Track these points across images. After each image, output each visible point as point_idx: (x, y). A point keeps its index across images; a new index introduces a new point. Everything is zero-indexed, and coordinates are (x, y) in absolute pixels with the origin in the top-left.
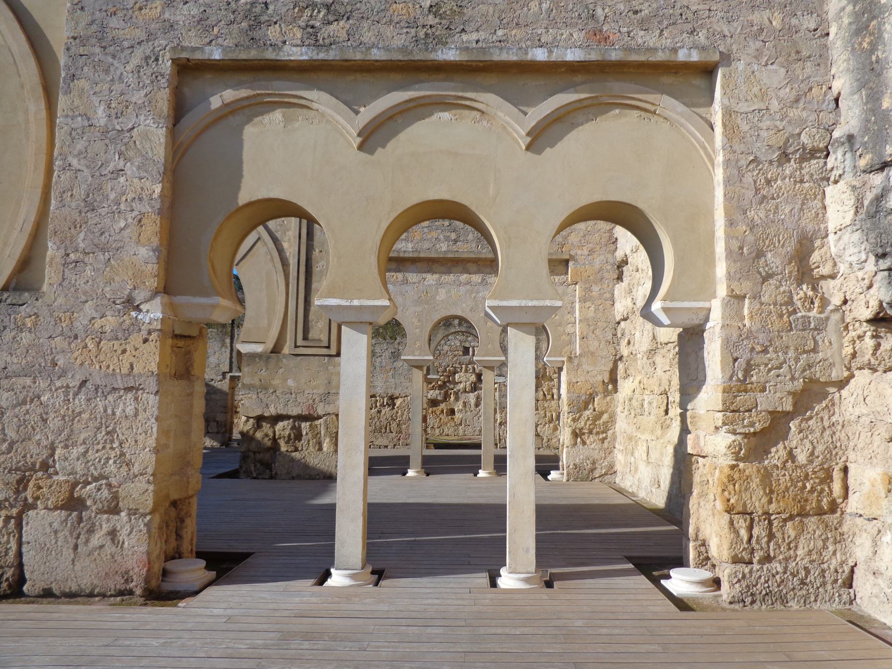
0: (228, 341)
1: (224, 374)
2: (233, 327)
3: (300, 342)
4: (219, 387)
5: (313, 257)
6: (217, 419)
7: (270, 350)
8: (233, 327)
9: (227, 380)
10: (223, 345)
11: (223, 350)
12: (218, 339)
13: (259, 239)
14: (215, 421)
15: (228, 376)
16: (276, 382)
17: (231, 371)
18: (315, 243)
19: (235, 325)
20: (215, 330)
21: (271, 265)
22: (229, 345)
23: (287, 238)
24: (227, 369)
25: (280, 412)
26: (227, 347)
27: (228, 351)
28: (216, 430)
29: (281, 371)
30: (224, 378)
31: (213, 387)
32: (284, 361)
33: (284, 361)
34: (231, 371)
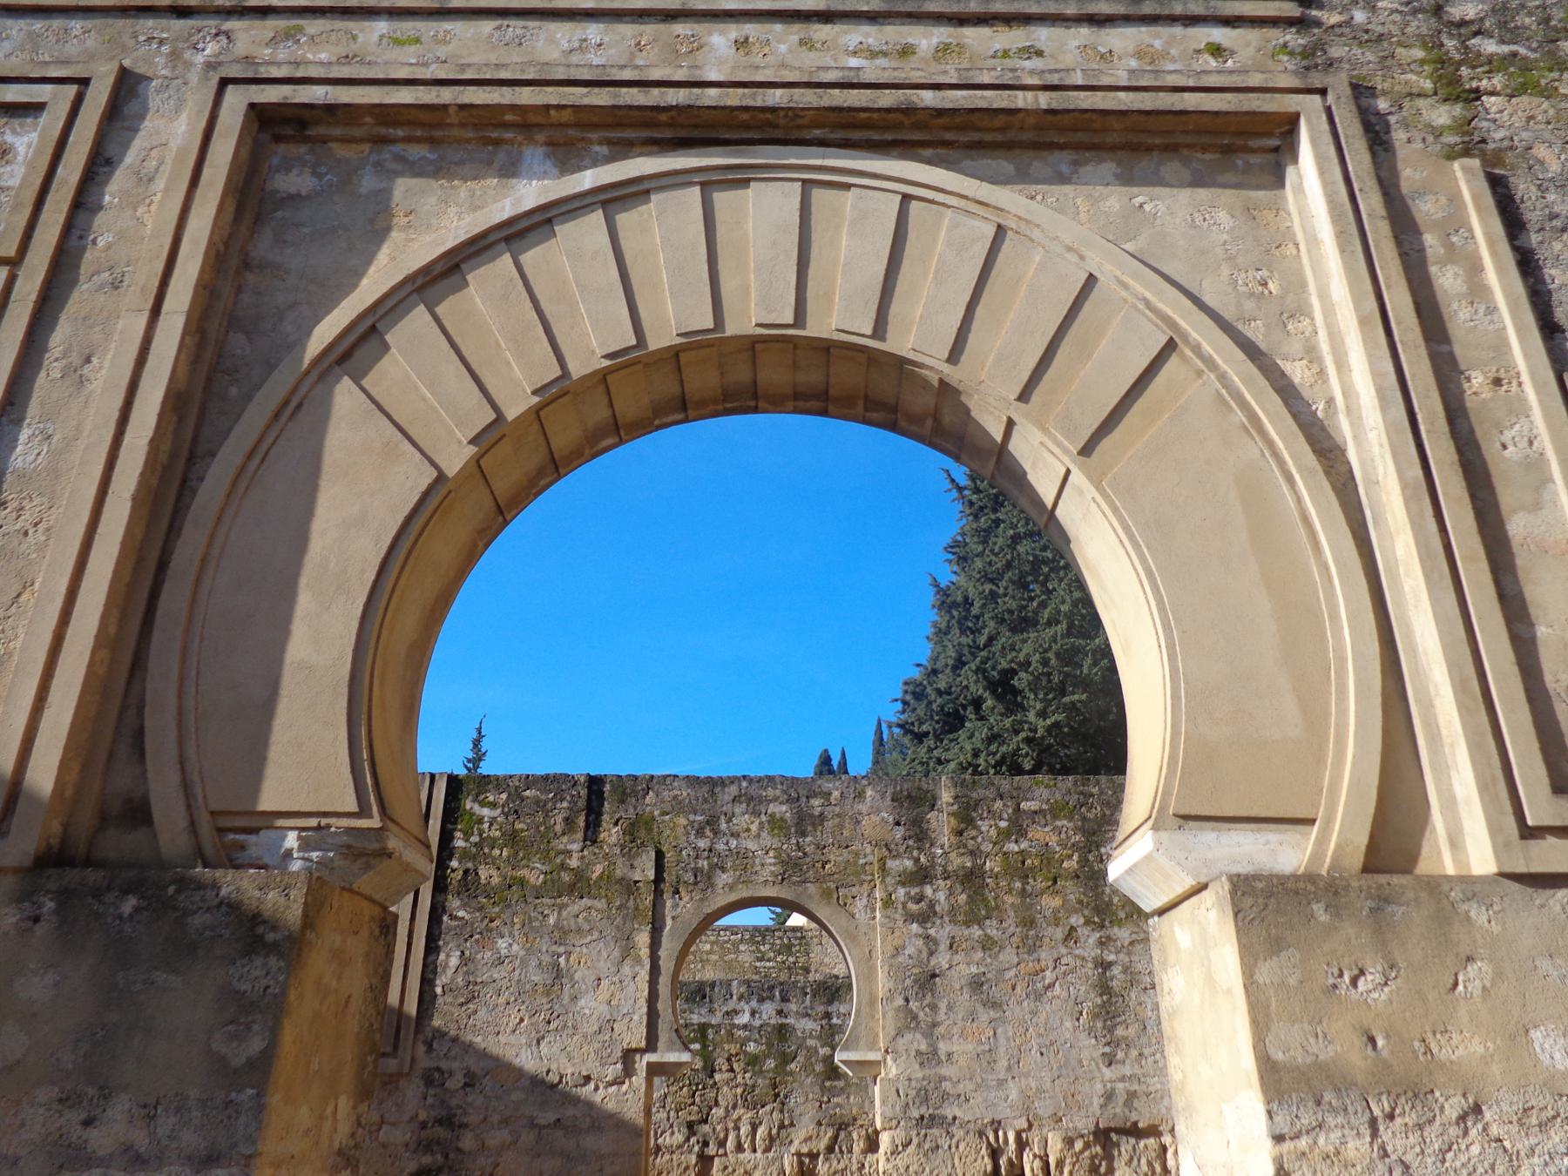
0: (643, 939)
1: (628, 1056)
2: (658, 893)
4: (611, 1106)
5: (1470, 402)
7: (1356, 860)
8: (658, 893)
9: (639, 1080)
10: (628, 951)
11: (626, 970)
12: (610, 932)
13: (1170, 346)
15: (642, 1062)
16: (1465, 1047)
17: (651, 1044)
18: (1458, 350)
19: (666, 887)
20: (601, 904)
21: (1252, 450)
22: (645, 952)
23: (1296, 347)
24: (638, 1038)
26: (638, 960)
27: (644, 974)
29: (1475, 977)
30: (628, 1071)
31: (590, 1105)
32: (1479, 915)
33: (1479, 915)
34: (651, 1044)
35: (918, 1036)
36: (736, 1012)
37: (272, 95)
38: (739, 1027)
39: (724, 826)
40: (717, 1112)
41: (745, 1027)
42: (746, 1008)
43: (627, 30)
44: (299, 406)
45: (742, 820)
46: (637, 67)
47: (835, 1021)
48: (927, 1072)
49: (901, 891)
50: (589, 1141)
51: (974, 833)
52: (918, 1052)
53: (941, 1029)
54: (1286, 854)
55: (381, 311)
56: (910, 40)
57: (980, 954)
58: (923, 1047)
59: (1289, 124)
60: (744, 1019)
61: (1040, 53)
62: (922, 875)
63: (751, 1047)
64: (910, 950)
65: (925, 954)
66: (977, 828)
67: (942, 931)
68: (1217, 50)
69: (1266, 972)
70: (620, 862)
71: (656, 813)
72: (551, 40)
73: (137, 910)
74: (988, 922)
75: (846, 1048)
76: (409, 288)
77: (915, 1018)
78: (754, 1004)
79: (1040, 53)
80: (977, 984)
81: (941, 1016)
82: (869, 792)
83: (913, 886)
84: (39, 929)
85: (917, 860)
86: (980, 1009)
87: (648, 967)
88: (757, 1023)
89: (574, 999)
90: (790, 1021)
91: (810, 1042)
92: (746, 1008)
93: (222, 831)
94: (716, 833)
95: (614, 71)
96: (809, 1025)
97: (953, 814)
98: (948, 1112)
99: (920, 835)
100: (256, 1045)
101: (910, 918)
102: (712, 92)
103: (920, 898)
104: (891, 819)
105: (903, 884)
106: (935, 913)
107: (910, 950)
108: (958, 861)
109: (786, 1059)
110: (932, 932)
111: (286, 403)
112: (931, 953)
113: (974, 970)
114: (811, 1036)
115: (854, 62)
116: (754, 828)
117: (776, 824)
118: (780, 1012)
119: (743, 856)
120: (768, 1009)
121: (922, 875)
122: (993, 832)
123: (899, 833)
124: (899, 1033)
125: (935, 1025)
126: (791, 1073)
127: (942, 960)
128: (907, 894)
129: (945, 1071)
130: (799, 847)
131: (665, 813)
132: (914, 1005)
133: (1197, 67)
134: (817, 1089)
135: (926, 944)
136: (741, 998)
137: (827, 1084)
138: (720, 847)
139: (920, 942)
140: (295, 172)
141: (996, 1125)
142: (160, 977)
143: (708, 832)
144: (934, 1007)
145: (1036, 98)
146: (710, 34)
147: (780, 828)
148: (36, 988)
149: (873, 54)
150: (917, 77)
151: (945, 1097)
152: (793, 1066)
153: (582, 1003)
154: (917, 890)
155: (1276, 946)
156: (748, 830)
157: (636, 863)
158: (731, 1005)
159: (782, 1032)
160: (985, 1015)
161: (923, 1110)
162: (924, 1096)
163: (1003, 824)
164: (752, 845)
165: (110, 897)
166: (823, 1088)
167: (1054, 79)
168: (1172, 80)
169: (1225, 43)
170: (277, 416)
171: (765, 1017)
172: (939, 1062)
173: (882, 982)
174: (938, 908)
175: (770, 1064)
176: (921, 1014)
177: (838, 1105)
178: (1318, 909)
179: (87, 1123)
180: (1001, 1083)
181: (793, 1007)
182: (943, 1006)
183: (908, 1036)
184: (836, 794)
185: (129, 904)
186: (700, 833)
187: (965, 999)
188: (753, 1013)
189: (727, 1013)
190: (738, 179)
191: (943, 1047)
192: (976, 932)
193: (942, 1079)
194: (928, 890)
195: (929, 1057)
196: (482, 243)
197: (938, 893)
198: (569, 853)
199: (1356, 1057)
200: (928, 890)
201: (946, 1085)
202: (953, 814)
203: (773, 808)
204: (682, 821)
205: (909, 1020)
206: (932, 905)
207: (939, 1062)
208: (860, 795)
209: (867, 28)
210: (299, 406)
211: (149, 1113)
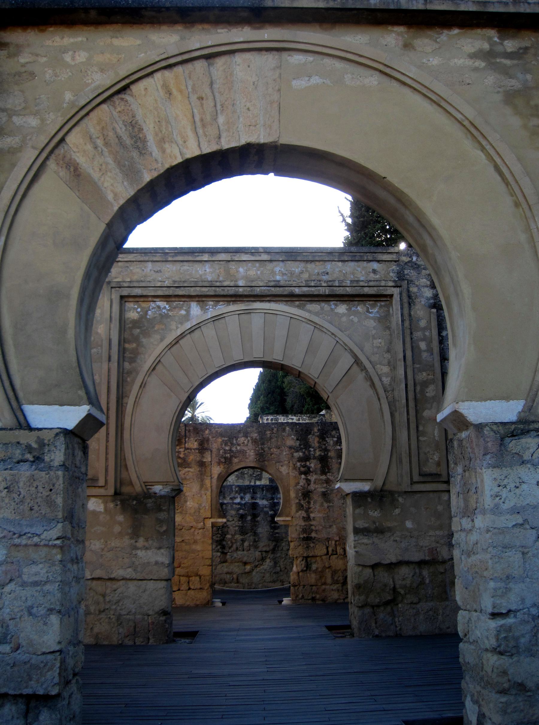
3: (416, 478)
6: (200, 573)
11: (203, 492)
14: (197, 575)
25: (400, 558)
28: (199, 586)
29: (397, 511)
32: (400, 499)
35: (303, 512)
36: (235, 498)
37: (125, 292)
38: (236, 504)
39: (235, 442)
40: (229, 536)
41: (239, 504)
42: (239, 496)
43: (216, 266)
44: (145, 383)
45: (242, 440)
46: (220, 282)
47: (275, 501)
48: (306, 523)
49: (298, 464)
50: (194, 547)
51: (325, 443)
52: (303, 517)
53: (311, 510)
54: (366, 487)
55: (161, 356)
56: (293, 269)
57: (325, 485)
58: (305, 515)
59: (391, 296)
60: (238, 500)
61: (327, 273)
62: (306, 458)
63: (241, 512)
64: (301, 484)
65: (306, 485)
66: (326, 441)
67: (313, 477)
68: (374, 271)
69: (357, 511)
70: (198, 455)
71: (210, 437)
72: (197, 271)
73: (136, 503)
74: (328, 474)
75: (279, 516)
76: (167, 349)
77: (302, 506)
78: (242, 495)
79: (327, 273)
80: (324, 495)
81: (312, 505)
82: (287, 429)
83: (302, 462)
84: (118, 507)
85: (304, 453)
86: (325, 503)
87: (210, 491)
88: (243, 502)
89: (186, 502)
90: (257, 501)
91: (265, 509)
92: (239, 496)
93: (146, 486)
94: (232, 444)
95: (214, 283)
96: (265, 502)
97: (318, 436)
98: (313, 535)
99: (305, 445)
100: (164, 528)
101: (301, 473)
102: (241, 290)
103: (304, 466)
104: (295, 438)
105: (299, 461)
106: (310, 471)
107: (301, 484)
108: (318, 453)
109: (255, 516)
110: (309, 478)
111: (142, 383)
112: (309, 485)
113: (323, 490)
114: (266, 507)
115: (278, 278)
116: (246, 442)
117: (255, 441)
118: (252, 498)
119: (243, 452)
120: (248, 498)
121: (306, 458)
122: (332, 442)
123: (298, 443)
124: (297, 512)
125: (309, 508)
126: (257, 522)
127: (312, 487)
128: (301, 465)
129: (312, 523)
130: (262, 449)
131: (213, 437)
132: (302, 502)
133: (369, 278)
134: (268, 527)
135: (306, 482)
136: (236, 492)
137: (273, 525)
138: (234, 449)
139: (305, 481)
140: (132, 311)
141: (328, 539)
142: (144, 516)
143: (229, 444)
144: (309, 503)
145: (325, 290)
146: (239, 268)
147: (255, 442)
148: (120, 518)
149: (284, 274)
150: (294, 284)
151: (312, 530)
152: (259, 519)
153: (188, 503)
154: (304, 463)
155: (360, 507)
156: (244, 443)
157: (204, 455)
158: (232, 495)
159: (254, 506)
160: (326, 505)
161: (305, 535)
162: (304, 531)
163: (335, 439)
164: (245, 448)
165: (131, 501)
166: (270, 526)
167: (330, 284)
168: (362, 284)
169: (378, 269)
170: (141, 386)
171: (246, 500)
172: (311, 520)
173: (292, 495)
174: (311, 469)
175: (249, 518)
176: (304, 505)
177: (277, 533)
178: (369, 500)
179: (136, 542)
180: (330, 526)
181: (258, 495)
182: (312, 502)
183: (300, 512)
184: (275, 429)
185: (135, 502)
186: (226, 445)
187: (320, 500)
188: (242, 498)
189: (231, 498)
190: (248, 312)
191: (312, 515)
192: (324, 477)
193: (312, 525)
194: (308, 463)
195: (307, 519)
196: (184, 335)
197: (313, 464)
198: (179, 452)
199: (373, 527)
200: (308, 463)
201: (313, 527)
202: (318, 436)
203: (252, 435)
204: (220, 440)
205: (300, 507)
206: (309, 468)
207: (311, 520)
208: (284, 430)
209: (281, 264)
210: (145, 383)
211: (147, 540)
